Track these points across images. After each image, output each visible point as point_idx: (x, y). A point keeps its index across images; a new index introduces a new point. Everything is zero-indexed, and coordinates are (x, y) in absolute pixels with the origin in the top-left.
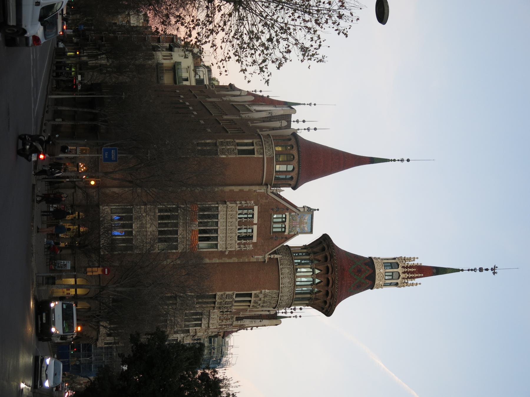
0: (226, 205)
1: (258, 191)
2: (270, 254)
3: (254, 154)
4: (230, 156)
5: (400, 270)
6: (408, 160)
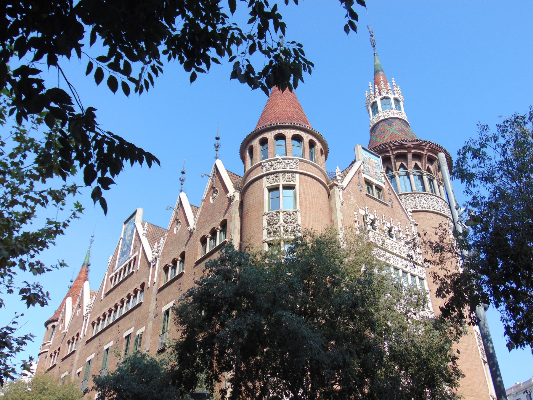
5: (392, 97)
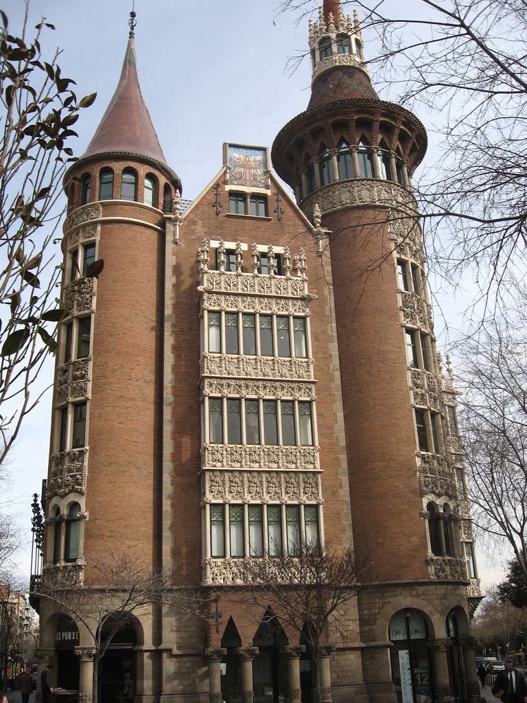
0: (206, 296)
1: (177, 237)
2: (314, 225)
3: (95, 240)
4: (95, 289)
6: (133, 15)
